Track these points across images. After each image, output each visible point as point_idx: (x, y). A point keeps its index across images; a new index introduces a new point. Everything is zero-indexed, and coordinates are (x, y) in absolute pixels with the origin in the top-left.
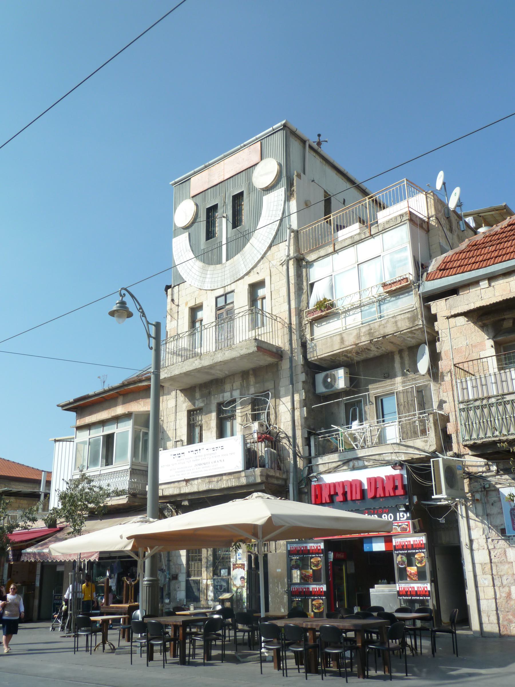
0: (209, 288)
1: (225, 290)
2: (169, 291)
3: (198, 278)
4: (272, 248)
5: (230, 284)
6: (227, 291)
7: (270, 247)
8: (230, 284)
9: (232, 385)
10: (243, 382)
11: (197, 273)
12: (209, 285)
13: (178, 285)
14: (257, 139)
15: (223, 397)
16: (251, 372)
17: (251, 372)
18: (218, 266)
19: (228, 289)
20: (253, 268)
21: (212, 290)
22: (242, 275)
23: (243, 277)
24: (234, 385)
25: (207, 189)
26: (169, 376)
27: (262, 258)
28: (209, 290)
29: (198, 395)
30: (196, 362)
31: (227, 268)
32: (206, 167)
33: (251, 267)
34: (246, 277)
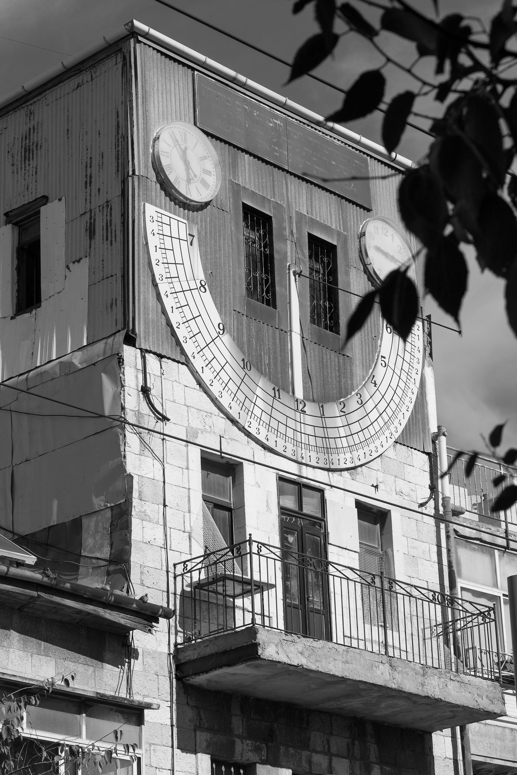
0: (262, 438)
5: (314, 467)
8: (314, 467)
9: (328, 742)
10: (353, 744)
13: (161, 356)
14: (358, 143)
15: (310, 762)
16: (369, 729)
17: (369, 729)
24: (333, 741)
25: (243, 150)
26: (313, 667)
28: (257, 441)
29: (238, 724)
30: (381, 666)
32: (233, 80)
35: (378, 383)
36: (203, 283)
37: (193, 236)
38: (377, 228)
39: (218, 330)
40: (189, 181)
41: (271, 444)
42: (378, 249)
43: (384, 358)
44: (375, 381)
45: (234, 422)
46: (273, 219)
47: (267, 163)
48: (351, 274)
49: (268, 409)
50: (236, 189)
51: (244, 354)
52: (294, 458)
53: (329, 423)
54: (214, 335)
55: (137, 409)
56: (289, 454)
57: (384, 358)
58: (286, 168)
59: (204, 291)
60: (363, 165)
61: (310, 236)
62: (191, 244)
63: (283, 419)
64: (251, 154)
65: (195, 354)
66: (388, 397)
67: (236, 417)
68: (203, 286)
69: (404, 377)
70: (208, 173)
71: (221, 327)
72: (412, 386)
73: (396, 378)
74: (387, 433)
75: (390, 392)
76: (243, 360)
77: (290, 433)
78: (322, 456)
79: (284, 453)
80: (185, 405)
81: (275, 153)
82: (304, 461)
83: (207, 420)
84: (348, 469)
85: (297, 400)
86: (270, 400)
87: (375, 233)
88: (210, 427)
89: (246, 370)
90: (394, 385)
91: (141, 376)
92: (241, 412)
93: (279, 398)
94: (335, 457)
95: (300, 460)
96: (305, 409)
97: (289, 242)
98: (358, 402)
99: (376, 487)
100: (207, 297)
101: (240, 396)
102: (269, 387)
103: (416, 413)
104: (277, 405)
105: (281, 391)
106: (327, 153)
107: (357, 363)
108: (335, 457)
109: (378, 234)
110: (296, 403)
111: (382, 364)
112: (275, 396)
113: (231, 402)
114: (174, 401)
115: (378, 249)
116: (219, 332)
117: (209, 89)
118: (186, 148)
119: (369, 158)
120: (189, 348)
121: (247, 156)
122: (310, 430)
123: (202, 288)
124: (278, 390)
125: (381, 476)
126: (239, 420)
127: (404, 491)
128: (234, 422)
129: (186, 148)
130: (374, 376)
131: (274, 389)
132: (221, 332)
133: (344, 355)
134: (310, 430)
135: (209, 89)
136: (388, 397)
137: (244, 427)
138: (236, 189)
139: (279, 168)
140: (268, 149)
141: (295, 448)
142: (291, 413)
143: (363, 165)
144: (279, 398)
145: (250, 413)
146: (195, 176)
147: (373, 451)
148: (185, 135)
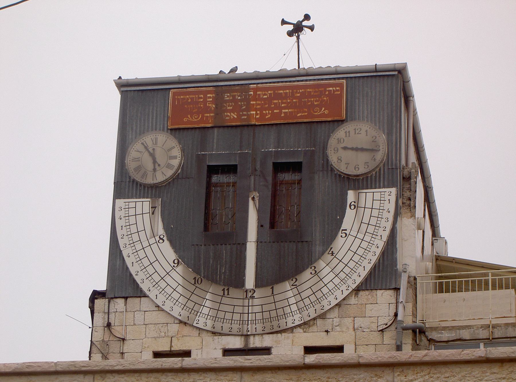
0: (209, 328)
1: (247, 342)
2: (100, 303)
3: (182, 300)
4: (361, 293)
5: (262, 334)
6: (251, 346)
7: (357, 290)
8: (262, 334)
11: (180, 289)
12: (210, 323)
13: (126, 298)
18: (234, 292)
19: (256, 342)
20: (314, 319)
21: (214, 333)
22: (290, 325)
23: (291, 330)
27: (338, 305)
28: (208, 331)
31: (256, 302)
33: (313, 315)
34: (300, 330)
35: (335, 252)
36: (162, 237)
37: (155, 207)
38: (349, 132)
39: (172, 264)
40: (155, 170)
41: (218, 329)
42: (345, 148)
43: (346, 230)
44: (332, 252)
45: (185, 323)
46: (238, 166)
47: (236, 126)
48: (316, 177)
49: (216, 306)
50: (200, 159)
51: (198, 273)
52: (240, 333)
53: (277, 298)
54: (168, 268)
55: (102, 339)
56: (234, 331)
57: (346, 230)
58: (253, 123)
59: (162, 241)
60: (338, 88)
61: (274, 164)
62: (153, 214)
63: (230, 308)
64: (220, 127)
65: (151, 289)
66: (345, 261)
67: (185, 320)
68: (162, 239)
69: (367, 238)
70: (175, 157)
71: (176, 262)
72: (376, 242)
73: (357, 241)
74: (344, 287)
75: (350, 254)
76: (195, 278)
77: (236, 317)
78: (268, 325)
79: (230, 333)
80: (144, 324)
81: (243, 117)
82: (249, 333)
83: (162, 330)
84: (299, 326)
85: (246, 291)
86: (218, 299)
87: (346, 136)
88: (165, 333)
89: (197, 285)
90: (354, 249)
91: (107, 316)
92: (190, 315)
93: (228, 294)
94: (282, 322)
95: (245, 333)
96: (255, 295)
97: (252, 178)
98: (311, 273)
99: (327, 331)
100: (166, 246)
101: (190, 304)
102: (219, 290)
103: (383, 260)
104: (225, 300)
105: (231, 289)
106: (299, 95)
107: (318, 242)
108: (282, 322)
109: (349, 136)
110: (245, 293)
111: (341, 236)
112: (224, 294)
113: (181, 311)
114: (134, 324)
115: (345, 148)
116: (174, 266)
117: (182, 97)
118: (154, 149)
119: (344, 81)
120: (144, 287)
121: (216, 130)
122: (257, 309)
123: (161, 241)
124: (228, 289)
125: (336, 321)
126: (188, 322)
127: (362, 325)
128: (185, 323)
129: (154, 149)
130: (331, 248)
131: (224, 290)
132: (176, 265)
133: (302, 242)
134: (257, 309)
135: (182, 97)
136: (345, 261)
137: (192, 326)
138: (200, 159)
139: (248, 126)
140: (235, 117)
141: (240, 327)
142: (240, 303)
143: (338, 88)
144: (228, 294)
145: (199, 313)
146: (159, 165)
147: (326, 306)
148: (156, 139)
